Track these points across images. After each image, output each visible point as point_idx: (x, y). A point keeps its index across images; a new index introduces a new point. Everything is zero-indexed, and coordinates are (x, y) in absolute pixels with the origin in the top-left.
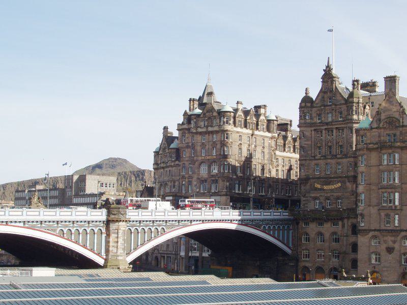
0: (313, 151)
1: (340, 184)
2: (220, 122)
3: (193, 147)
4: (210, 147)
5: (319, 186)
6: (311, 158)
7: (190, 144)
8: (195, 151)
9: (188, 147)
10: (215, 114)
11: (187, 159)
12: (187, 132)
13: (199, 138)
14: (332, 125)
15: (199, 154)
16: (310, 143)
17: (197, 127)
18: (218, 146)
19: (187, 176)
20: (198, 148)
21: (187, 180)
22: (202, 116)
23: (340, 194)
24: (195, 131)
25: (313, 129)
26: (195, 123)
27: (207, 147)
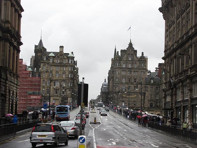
0: (121, 80)
1: (135, 96)
2: (68, 61)
3: (51, 72)
4: (62, 73)
5: (125, 96)
6: (121, 83)
7: (49, 71)
8: (52, 75)
9: (47, 72)
10: (65, 57)
11: (46, 78)
12: (46, 64)
13: (54, 68)
14: (132, 69)
15: (54, 76)
16: (120, 76)
17: (53, 62)
18: (67, 73)
19: (45, 86)
20: (54, 73)
21: (46, 88)
22: (56, 57)
23: (136, 100)
24: (52, 64)
25: (121, 70)
26: (53, 60)
27: (60, 73)
